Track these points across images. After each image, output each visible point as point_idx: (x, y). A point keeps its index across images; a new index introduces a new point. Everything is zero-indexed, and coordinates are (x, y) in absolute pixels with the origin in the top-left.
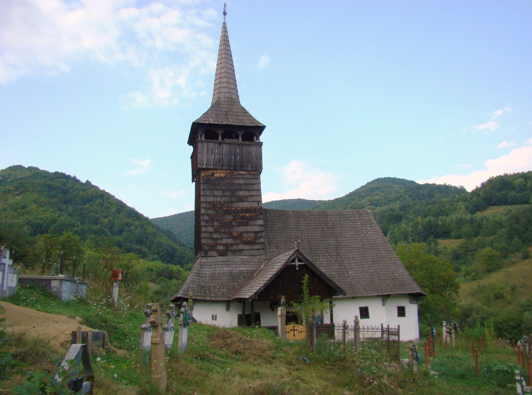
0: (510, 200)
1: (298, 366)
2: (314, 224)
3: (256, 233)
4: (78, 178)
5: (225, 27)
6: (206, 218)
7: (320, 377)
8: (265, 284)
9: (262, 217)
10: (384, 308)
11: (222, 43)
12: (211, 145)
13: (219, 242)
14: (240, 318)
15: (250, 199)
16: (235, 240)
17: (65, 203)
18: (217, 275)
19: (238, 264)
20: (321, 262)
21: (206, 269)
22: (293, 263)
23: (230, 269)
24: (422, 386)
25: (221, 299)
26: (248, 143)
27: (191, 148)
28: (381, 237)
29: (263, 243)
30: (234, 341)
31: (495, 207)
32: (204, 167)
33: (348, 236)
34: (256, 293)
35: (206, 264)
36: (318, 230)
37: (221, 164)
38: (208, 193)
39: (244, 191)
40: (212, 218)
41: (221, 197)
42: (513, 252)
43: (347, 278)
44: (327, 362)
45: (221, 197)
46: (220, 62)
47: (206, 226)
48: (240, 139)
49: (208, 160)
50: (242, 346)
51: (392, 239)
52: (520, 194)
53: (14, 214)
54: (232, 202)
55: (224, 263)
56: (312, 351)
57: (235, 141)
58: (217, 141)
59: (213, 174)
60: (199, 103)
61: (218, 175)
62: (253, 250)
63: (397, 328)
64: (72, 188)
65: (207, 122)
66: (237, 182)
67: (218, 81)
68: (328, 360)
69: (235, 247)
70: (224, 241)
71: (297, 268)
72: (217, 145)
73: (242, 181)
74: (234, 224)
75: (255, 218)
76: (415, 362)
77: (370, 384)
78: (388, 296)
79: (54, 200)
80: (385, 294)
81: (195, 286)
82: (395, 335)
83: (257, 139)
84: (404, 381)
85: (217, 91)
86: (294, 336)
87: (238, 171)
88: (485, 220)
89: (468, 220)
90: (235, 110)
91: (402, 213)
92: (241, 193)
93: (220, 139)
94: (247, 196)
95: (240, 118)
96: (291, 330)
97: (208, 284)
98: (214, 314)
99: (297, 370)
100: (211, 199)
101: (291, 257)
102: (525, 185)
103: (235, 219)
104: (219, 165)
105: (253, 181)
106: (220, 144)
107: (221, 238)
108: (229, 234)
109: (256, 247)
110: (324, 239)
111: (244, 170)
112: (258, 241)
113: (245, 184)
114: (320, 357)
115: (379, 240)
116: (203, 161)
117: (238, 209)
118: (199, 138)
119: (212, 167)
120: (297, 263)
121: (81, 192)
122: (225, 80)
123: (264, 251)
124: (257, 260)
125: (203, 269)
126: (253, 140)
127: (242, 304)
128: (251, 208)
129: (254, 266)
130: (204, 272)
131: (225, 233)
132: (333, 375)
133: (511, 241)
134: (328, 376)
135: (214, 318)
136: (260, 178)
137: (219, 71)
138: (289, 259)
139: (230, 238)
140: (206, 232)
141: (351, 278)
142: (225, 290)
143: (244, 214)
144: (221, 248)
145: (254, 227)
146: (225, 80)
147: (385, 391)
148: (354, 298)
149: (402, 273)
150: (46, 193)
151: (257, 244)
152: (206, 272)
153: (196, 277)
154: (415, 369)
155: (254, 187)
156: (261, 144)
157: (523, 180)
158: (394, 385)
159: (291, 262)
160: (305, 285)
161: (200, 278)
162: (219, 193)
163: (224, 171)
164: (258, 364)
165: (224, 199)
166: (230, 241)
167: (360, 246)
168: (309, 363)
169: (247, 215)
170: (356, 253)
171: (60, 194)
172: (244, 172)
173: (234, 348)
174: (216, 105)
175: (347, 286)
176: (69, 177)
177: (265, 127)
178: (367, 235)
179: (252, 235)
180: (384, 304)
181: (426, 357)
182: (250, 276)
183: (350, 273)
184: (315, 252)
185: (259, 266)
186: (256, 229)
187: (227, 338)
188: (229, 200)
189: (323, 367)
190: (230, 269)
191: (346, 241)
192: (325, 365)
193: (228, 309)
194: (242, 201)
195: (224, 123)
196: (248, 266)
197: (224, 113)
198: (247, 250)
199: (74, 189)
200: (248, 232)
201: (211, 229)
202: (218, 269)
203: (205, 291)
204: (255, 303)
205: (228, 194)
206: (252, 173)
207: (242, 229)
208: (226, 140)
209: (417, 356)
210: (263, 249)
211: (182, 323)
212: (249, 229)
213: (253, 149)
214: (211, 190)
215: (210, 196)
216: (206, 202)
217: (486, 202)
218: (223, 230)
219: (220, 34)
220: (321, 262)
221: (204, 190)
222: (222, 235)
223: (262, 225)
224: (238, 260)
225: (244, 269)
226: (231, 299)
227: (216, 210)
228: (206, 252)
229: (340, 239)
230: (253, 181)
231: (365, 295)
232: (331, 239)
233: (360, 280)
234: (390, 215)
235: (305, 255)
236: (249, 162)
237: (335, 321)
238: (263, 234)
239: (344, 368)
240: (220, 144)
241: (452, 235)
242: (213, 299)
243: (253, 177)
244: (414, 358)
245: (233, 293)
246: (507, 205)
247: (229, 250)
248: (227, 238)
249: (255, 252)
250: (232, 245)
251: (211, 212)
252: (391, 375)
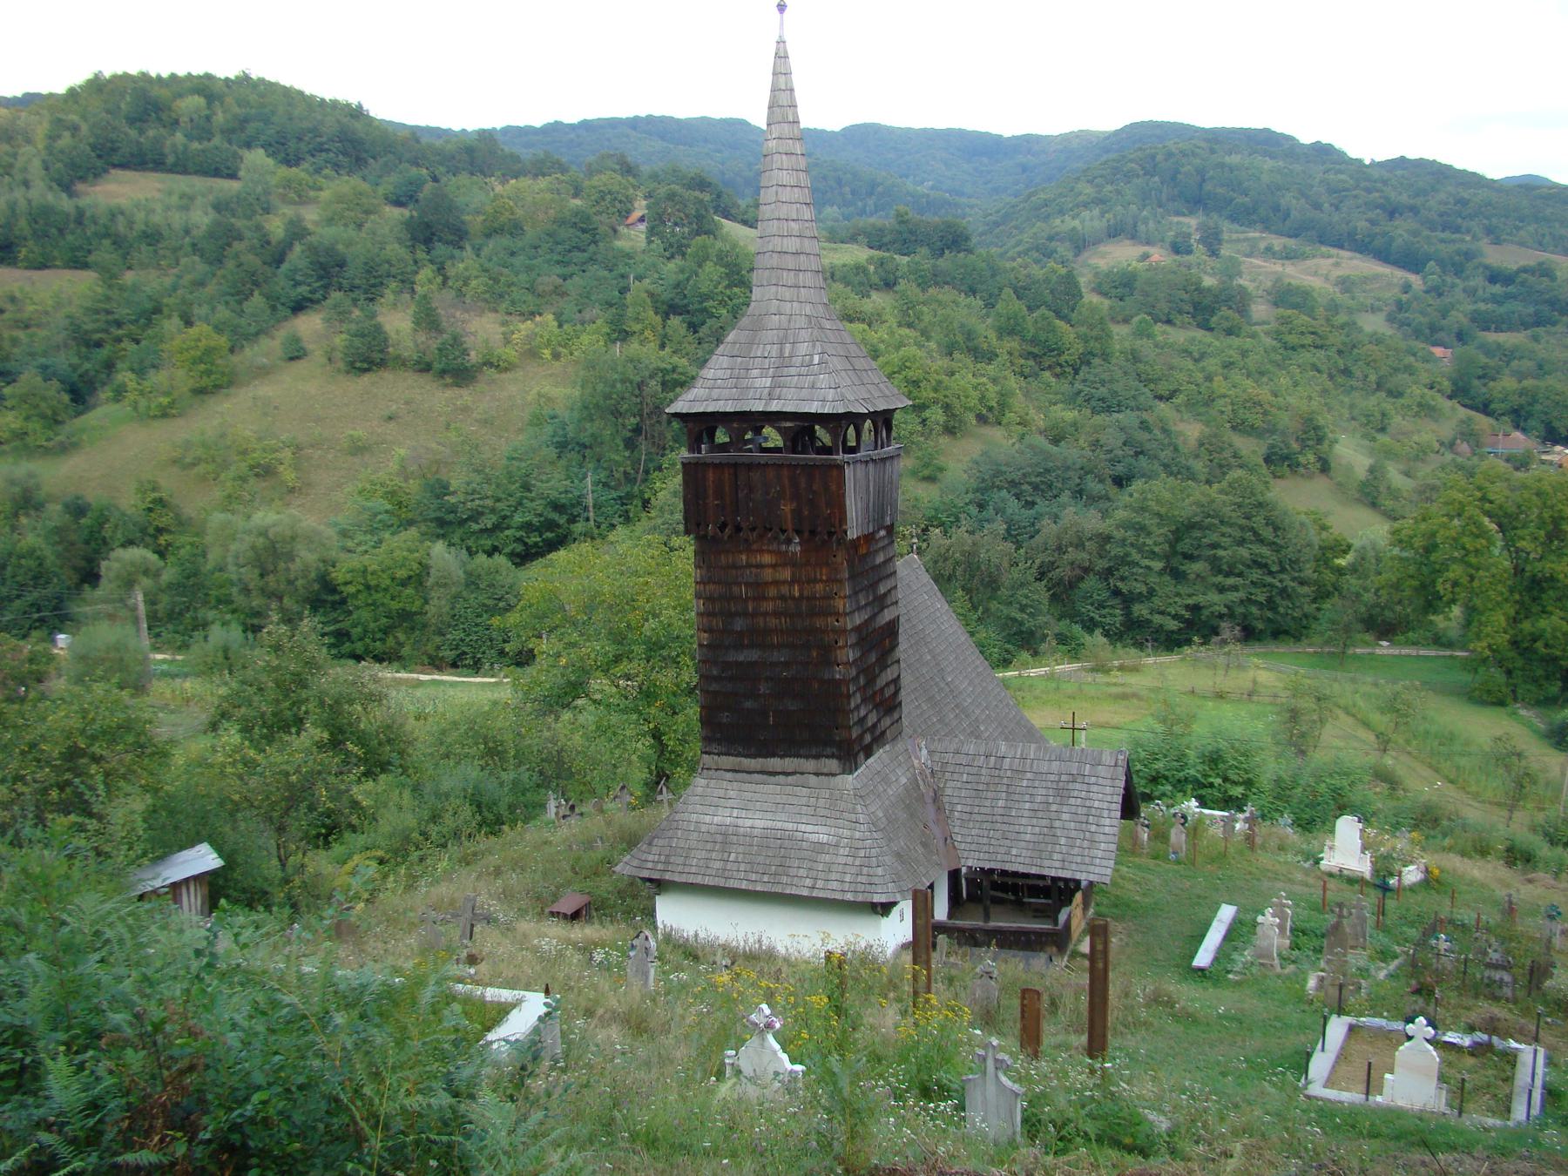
0: (170, 160)
31: (129, 174)
52: (196, 145)
88: (120, 218)
89: (68, 215)
217: (99, 157)
241: (21, 256)
246: (162, 171)
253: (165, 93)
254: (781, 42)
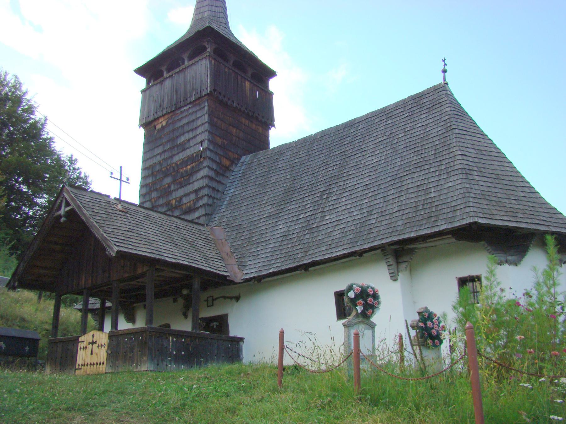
3: (196, 191)
15: (192, 143)
39: (187, 134)
54: (172, 157)
61: (159, 127)
66: (178, 125)
73: (185, 121)
87: (179, 108)
92: (182, 139)
94: (189, 140)
96: (89, 343)
111: (188, 104)
112: (200, 203)
113: (188, 123)
117: (179, 163)
128: (193, 154)
151: (199, 208)
163: (166, 117)
169: (189, 167)
172: (188, 107)
186: (196, 185)
194: (184, 150)
200: (187, 195)
206: (197, 102)
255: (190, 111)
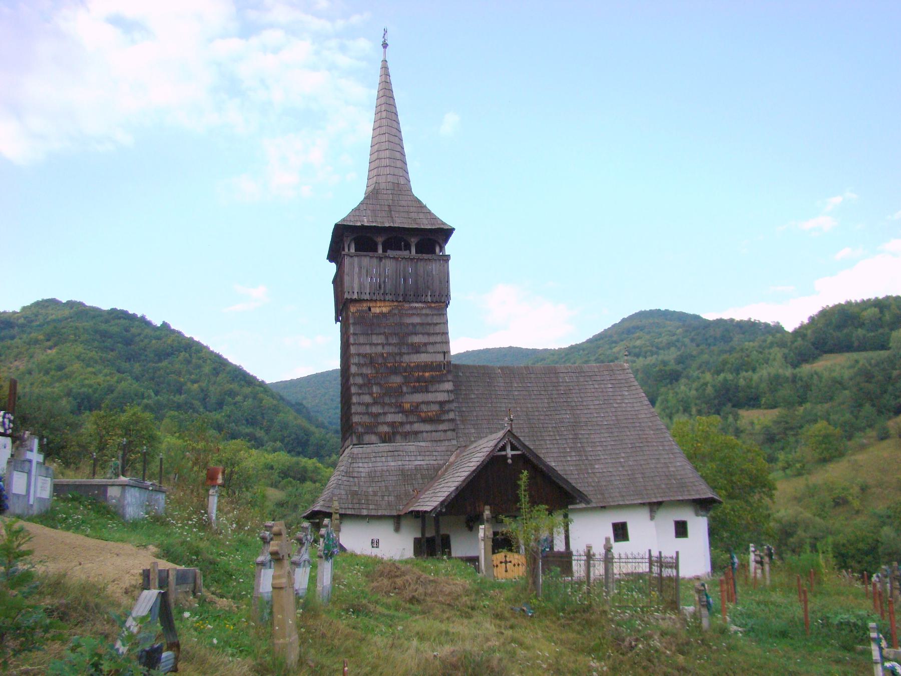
0: (856, 344)
1: (513, 621)
2: (536, 389)
3: (442, 403)
4: (148, 318)
5: (385, 68)
6: (359, 380)
7: (550, 639)
8: (457, 488)
9: (450, 377)
10: (652, 523)
11: (381, 93)
12: (366, 261)
13: (381, 419)
14: (418, 543)
15: (430, 349)
16: (407, 416)
17: (128, 359)
18: (378, 474)
19: (413, 454)
20: (549, 450)
21: (361, 465)
22: (503, 453)
23: (400, 463)
24: (718, 650)
25: (386, 513)
26: (425, 256)
27: (332, 268)
28: (645, 407)
29: (452, 420)
30: (407, 581)
31: (833, 355)
32: (355, 296)
33: (592, 407)
34: (442, 503)
35: (360, 456)
36: (542, 397)
37: (382, 291)
38: (362, 339)
39: (420, 336)
40: (369, 380)
41: (383, 345)
42: (862, 429)
43: (592, 475)
44: (561, 614)
45: (383, 345)
46: (378, 124)
47: (359, 394)
48: (413, 250)
49: (361, 285)
50: (421, 590)
51: (664, 410)
52: (872, 334)
53: (45, 378)
54: (401, 354)
55: (389, 454)
56: (536, 596)
57: (405, 253)
58: (376, 254)
59: (370, 309)
60: (345, 194)
61: (378, 310)
62: (436, 431)
63: (674, 555)
64: (139, 334)
65: (359, 224)
66: (409, 320)
67: (375, 156)
68: (563, 610)
69: (408, 428)
70: (390, 418)
71: (510, 461)
72: (375, 261)
73: (416, 320)
74: (405, 389)
75: (441, 381)
76: (704, 611)
77: (632, 648)
78: (659, 504)
79: (111, 355)
80: (655, 500)
81: (343, 492)
82: (671, 567)
83: (441, 251)
84: (688, 643)
85: (375, 172)
86: (506, 571)
87: (410, 302)
88: (815, 376)
90: (403, 203)
91: (679, 368)
92: (416, 339)
93: (380, 251)
94: (425, 344)
95: (413, 215)
96: (501, 562)
97: (364, 489)
98: (375, 538)
99: (512, 627)
100: (367, 350)
101: (499, 443)
102: (880, 319)
103: (406, 382)
104: (379, 293)
105: (436, 320)
106: (380, 259)
107: (385, 414)
108: (397, 407)
109: (442, 427)
110: (553, 413)
113: (422, 324)
114: (550, 605)
115: (642, 412)
116: (353, 288)
117: (412, 365)
118: (346, 250)
119: (367, 297)
120: (509, 453)
121: (154, 341)
122: (387, 154)
123: (454, 434)
124: (444, 449)
125: (355, 465)
126: (434, 252)
127: (419, 521)
129: (439, 458)
130: (356, 469)
131: (390, 405)
132: (571, 636)
133: (859, 411)
134: (563, 636)
135: (375, 543)
136: (446, 314)
137: (376, 140)
138: (496, 446)
139: (399, 413)
140: (359, 404)
141: (598, 475)
142: (392, 498)
143: (421, 374)
144: (385, 429)
145: (438, 394)
146: (387, 154)
147: (656, 660)
148: (604, 507)
149: (681, 466)
150: (96, 344)
151: (444, 421)
152: (361, 470)
153: (345, 478)
154: (705, 623)
155: (437, 329)
156: (447, 258)
157: (877, 310)
158: (670, 650)
159: (499, 451)
160: (523, 488)
161: (351, 479)
162: (380, 339)
163: (387, 304)
164: (448, 618)
165: (388, 349)
166: (399, 418)
167: (611, 422)
168: (531, 616)
169: (427, 374)
170: (606, 435)
171: (120, 345)
172: (420, 305)
173: (407, 594)
174: (373, 195)
175: (591, 488)
176: (133, 317)
177: (454, 229)
178: (624, 405)
179: (436, 408)
180: (652, 518)
181: (723, 603)
182: (433, 475)
183: (597, 466)
184: (539, 434)
185: (446, 457)
186: (442, 397)
187: (397, 576)
188: (396, 350)
189: (554, 622)
190: (400, 463)
191: (589, 416)
192: (558, 619)
193: (397, 529)
194: (418, 352)
195: (387, 225)
196: (430, 458)
197: (386, 208)
198: (427, 432)
199: (142, 337)
200: (428, 403)
201: (367, 399)
202: (380, 464)
203: (359, 500)
204: (441, 518)
205: (394, 341)
206: (433, 305)
207: (418, 398)
208: (390, 253)
209: (708, 602)
210: (454, 430)
211: (322, 553)
212: (430, 397)
213: (434, 267)
214: (367, 334)
215: (366, 344)
216: (359, 355)
217: (817, 348)
218: (387, 400)
219: (377, 80)
220: (549, 450)
221: (354, 334)
222: (386, 409)
223: (451, 391)
224: (412, 448)
225: (422, 463)
226: (402, 513)
227: (375, 367)
228: (360, 436)
229: (578, 412)
230: (436, 320)
231: (621, 503)
232: (564, 412)
233: (613, 478)
234: (661, 371)
235: (522, 439)
236: (428, 287)
237: (573, 547)
238: (453, 406)
239: (589, 624)
240: (380, 259)
241: (763, 402)
242: (373, 513)
243: (436, 312)
244: (703, 606)
245: (405, 503)
246: (852, 351)
247: (398, 432)
248: (394, 413)
249: (440, 435)
250: (402, 424)
251: (367, 371)
252: (666, 634)
253: (857, 310)
254: (385, 61)
255: (424, 312)
